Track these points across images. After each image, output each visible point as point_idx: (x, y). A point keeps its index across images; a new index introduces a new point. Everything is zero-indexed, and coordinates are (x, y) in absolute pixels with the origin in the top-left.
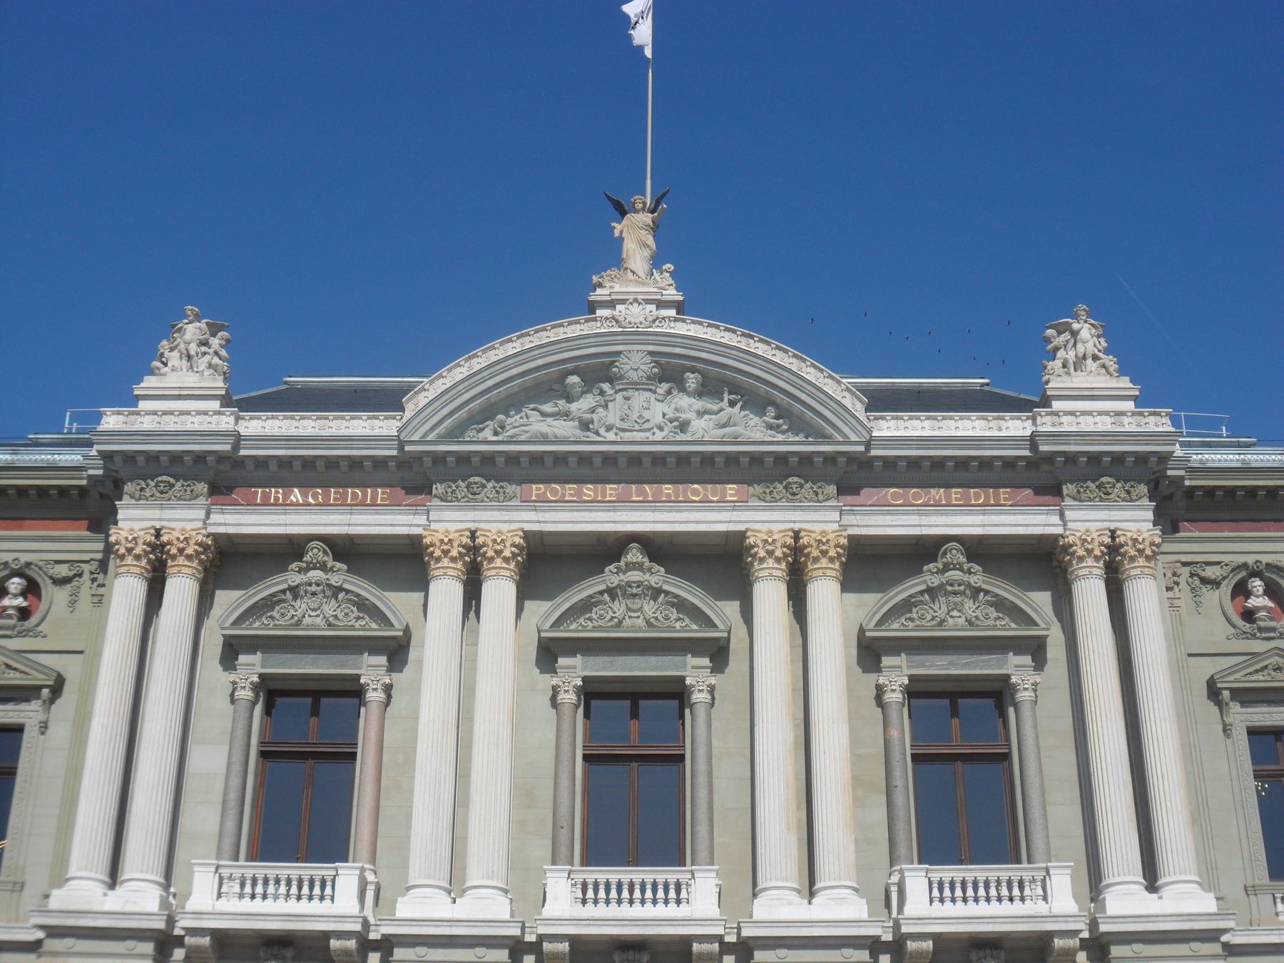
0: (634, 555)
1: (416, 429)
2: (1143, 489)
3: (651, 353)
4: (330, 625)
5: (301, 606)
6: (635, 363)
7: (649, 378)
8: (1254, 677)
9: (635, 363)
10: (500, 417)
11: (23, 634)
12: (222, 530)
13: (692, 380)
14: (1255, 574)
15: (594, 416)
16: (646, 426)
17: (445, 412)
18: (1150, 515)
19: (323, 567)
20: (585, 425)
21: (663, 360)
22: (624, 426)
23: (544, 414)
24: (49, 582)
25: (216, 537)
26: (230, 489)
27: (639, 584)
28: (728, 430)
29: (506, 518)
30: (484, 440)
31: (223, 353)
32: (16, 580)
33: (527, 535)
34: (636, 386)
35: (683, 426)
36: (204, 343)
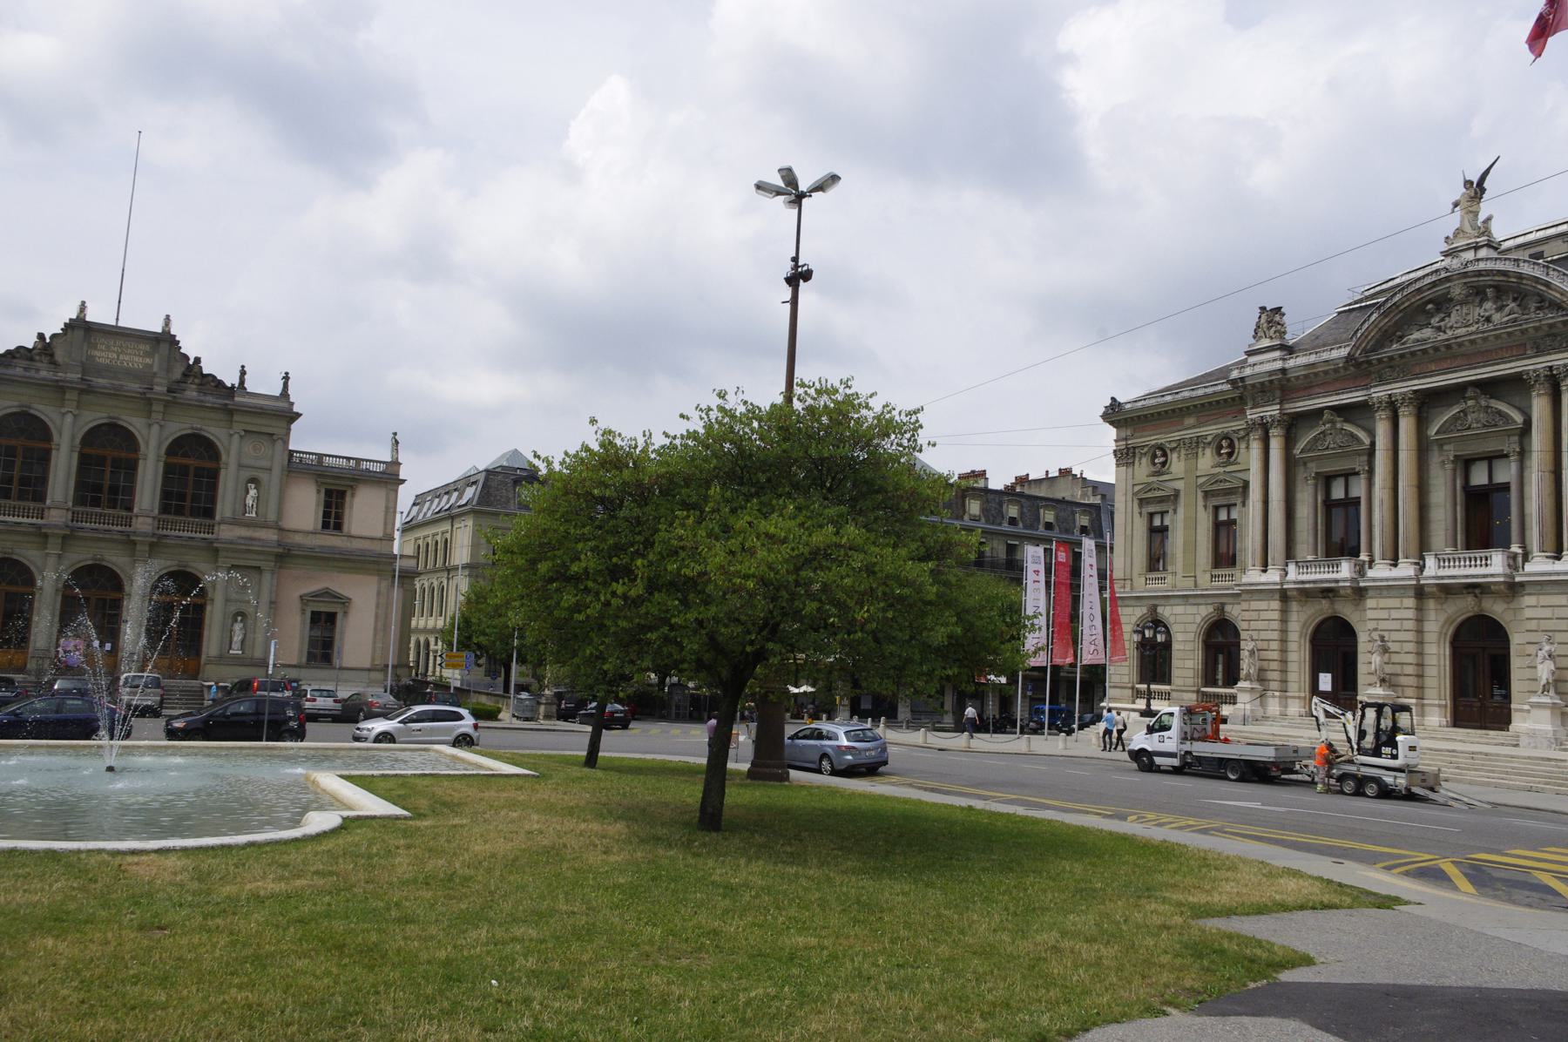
0: (1470, 393)
6: (1457, 291)
9: (1457, 291)
12: (1289, 411)
15: (1442, 324)
28: (1511, 317)
33: (1415, 392)
35: (1488, 320)
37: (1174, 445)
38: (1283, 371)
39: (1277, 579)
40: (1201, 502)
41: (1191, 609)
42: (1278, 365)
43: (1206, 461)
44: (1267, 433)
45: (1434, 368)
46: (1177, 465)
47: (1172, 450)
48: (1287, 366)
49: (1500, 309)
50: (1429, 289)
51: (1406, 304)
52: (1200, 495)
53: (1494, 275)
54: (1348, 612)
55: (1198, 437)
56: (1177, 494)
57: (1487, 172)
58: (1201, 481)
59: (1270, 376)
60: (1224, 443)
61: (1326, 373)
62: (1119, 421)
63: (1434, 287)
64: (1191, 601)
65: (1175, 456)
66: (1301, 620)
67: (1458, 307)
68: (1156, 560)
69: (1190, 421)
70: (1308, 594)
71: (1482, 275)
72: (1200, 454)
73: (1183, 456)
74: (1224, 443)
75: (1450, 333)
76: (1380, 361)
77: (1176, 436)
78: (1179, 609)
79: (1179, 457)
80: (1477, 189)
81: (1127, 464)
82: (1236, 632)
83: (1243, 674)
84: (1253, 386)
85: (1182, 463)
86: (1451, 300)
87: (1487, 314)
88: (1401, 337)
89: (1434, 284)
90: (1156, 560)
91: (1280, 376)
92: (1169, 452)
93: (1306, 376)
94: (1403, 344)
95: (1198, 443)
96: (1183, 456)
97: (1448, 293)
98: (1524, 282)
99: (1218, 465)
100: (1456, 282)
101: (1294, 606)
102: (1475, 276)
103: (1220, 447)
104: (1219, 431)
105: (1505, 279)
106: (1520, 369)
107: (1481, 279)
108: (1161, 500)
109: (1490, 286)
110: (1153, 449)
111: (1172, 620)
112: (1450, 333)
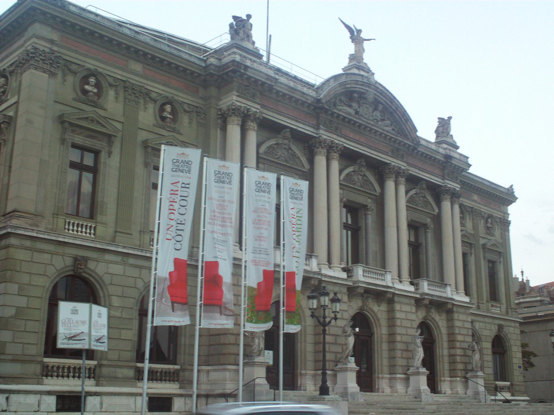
13: (380, 107)
20: (357, 113)
21: (376, 97)
22: (365, 116)
24: (182, 111)
29: (338, 139)
45: (352, 136)
50: (360, 85)
51: (349, 86)
53: (387, 99)
59: (267, 79)
60: (168, 108)
61: (297, 100)
63: (362, 85)
64: (131, 261)
67: (367, 106)
69: (138, 67)
71: (382, 94)
74: (168, 108)
76: (333, 113)
77: (119, 74)
80: (374, 39)
81: (52, 75)
84: (249, 78)
86: (365, 99)
89: (363, 84)
91: (273, 84)
92: (104, 84)
93: (284, 95)
98: (398, 112)
100: (372, 91)
102: (379, 93)
104: (170, 95)
105: (390, 104)
106: (389, 162)
107: (381, 97)
109: (382, 104)
110: (85, 73)
111: (107, 279)
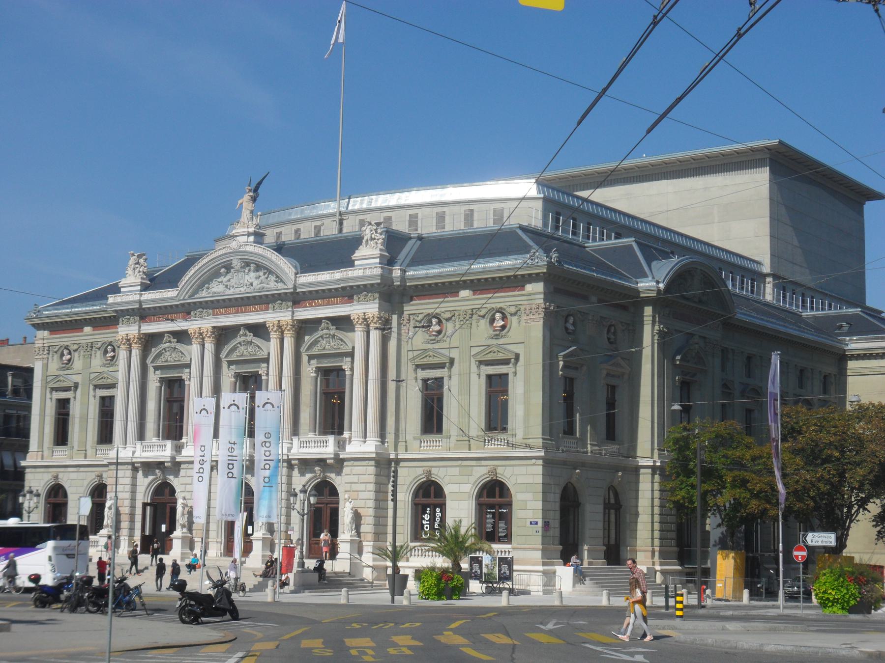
1: (182, 295)
2: (377, 295)
3: (240, 259)
4: (175, 360)
5: (168, 353)
6: (236, 263)
7: (241, 267)
8: (422, 360)
10: (206, 285)
11: (112, 365)
12: (146, 332)
14: (435, 317)
16: (242, 285)
17: (188, 288)
18: (377, 305)
19: (170, 342)
20: (226, 286)
23: (219, 282)
25: (145, 334)
26: (146, 317)
27: (244, 341)
30: (204, 295)
31: (146, 264)
32: (109, 347)
33: (214, 327)
34: (237, 271)
35: (252, 284)
36: (138, 263)
37: (76, 347)
38: (140, 302)
39: (130, 455)
40: (92, 392)
41: (81, 476)
42: (137, 297)
43: (97, 361)
44: (130, 345)
46: (78, 364)
47: (75, 351)
48: (142, 299)
49: (258, 278)
52: (92, 387)
54: (172, 479)
55: (92, 343)
56: (76, 386)
57: (260, 183)
58: (93, 376)
62: (38, 324)
65: (76, 354)
66: (145, 484)
68: (61, 437)
70: (149, 467)
72: (93, 355)
73: (81, 356)
75: (232, 290)
78: (73, 476)
79: (79, 357)
82: (65, 495)
83: (105, 523)
85: (81, 362)
87: (250, 281)
88: (208, 288)
90: (61, 437)
94: (209, 293)
95: (92, 347)
96: (81, 356)
97: (231, 264)
99: (104, 365)
101: (140, 474)
103: (106, 352)
108: (66, 389)
110: (62, 349)
112: (232, 290)
